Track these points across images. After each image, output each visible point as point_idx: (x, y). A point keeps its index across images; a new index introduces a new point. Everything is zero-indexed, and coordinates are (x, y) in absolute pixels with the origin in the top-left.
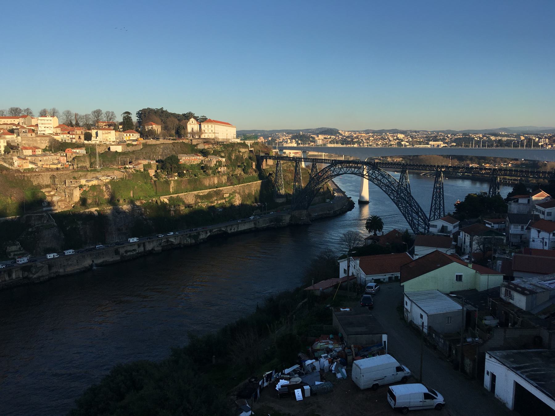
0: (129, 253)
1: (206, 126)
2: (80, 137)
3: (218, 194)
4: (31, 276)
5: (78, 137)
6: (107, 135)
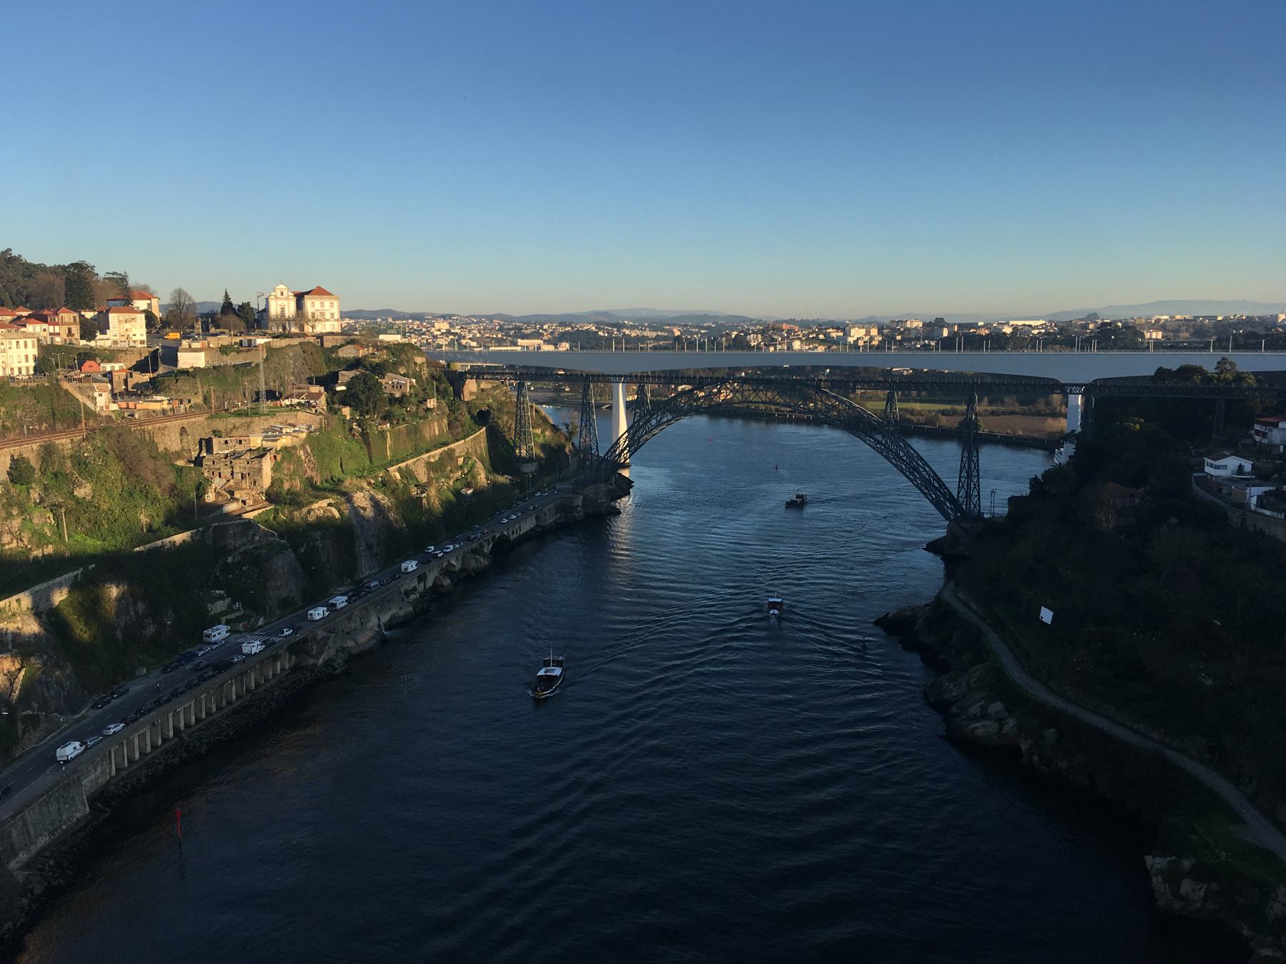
0: (413, 597)
1: (317, 304)
2: (70, 330)
3: (450, 455)
4: (311, 661)
5: (66, 328)
6: (128, 326)
